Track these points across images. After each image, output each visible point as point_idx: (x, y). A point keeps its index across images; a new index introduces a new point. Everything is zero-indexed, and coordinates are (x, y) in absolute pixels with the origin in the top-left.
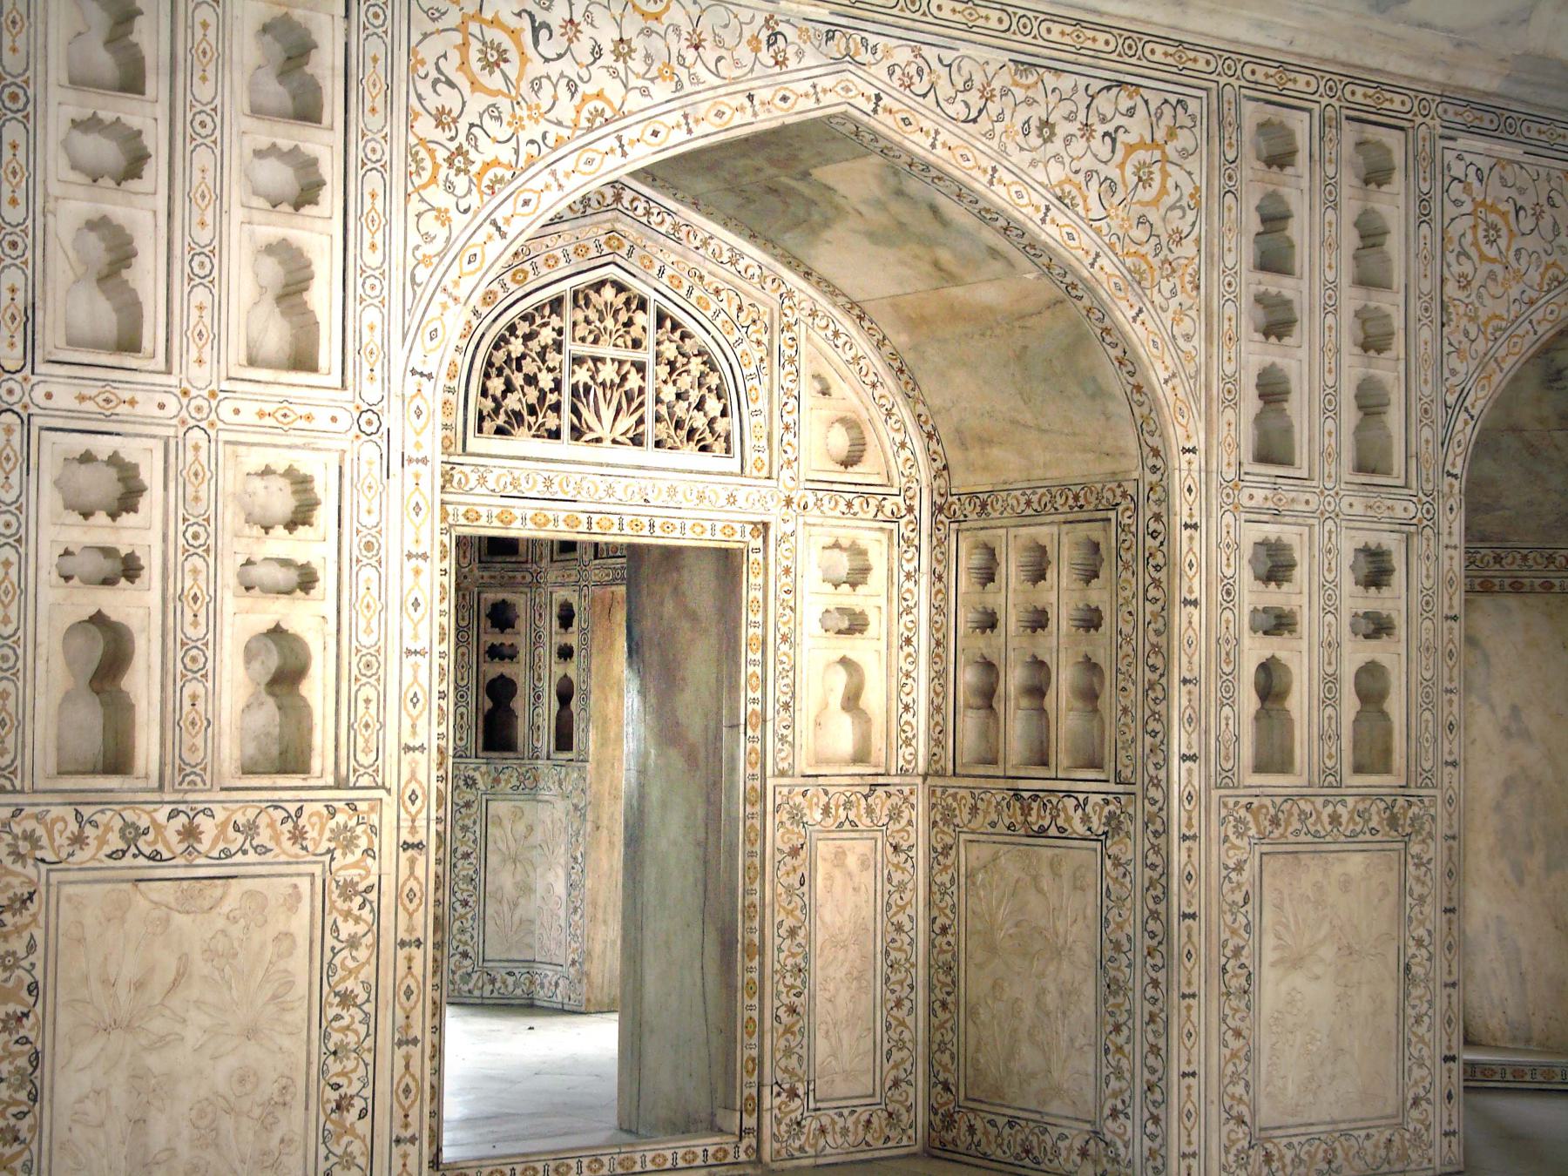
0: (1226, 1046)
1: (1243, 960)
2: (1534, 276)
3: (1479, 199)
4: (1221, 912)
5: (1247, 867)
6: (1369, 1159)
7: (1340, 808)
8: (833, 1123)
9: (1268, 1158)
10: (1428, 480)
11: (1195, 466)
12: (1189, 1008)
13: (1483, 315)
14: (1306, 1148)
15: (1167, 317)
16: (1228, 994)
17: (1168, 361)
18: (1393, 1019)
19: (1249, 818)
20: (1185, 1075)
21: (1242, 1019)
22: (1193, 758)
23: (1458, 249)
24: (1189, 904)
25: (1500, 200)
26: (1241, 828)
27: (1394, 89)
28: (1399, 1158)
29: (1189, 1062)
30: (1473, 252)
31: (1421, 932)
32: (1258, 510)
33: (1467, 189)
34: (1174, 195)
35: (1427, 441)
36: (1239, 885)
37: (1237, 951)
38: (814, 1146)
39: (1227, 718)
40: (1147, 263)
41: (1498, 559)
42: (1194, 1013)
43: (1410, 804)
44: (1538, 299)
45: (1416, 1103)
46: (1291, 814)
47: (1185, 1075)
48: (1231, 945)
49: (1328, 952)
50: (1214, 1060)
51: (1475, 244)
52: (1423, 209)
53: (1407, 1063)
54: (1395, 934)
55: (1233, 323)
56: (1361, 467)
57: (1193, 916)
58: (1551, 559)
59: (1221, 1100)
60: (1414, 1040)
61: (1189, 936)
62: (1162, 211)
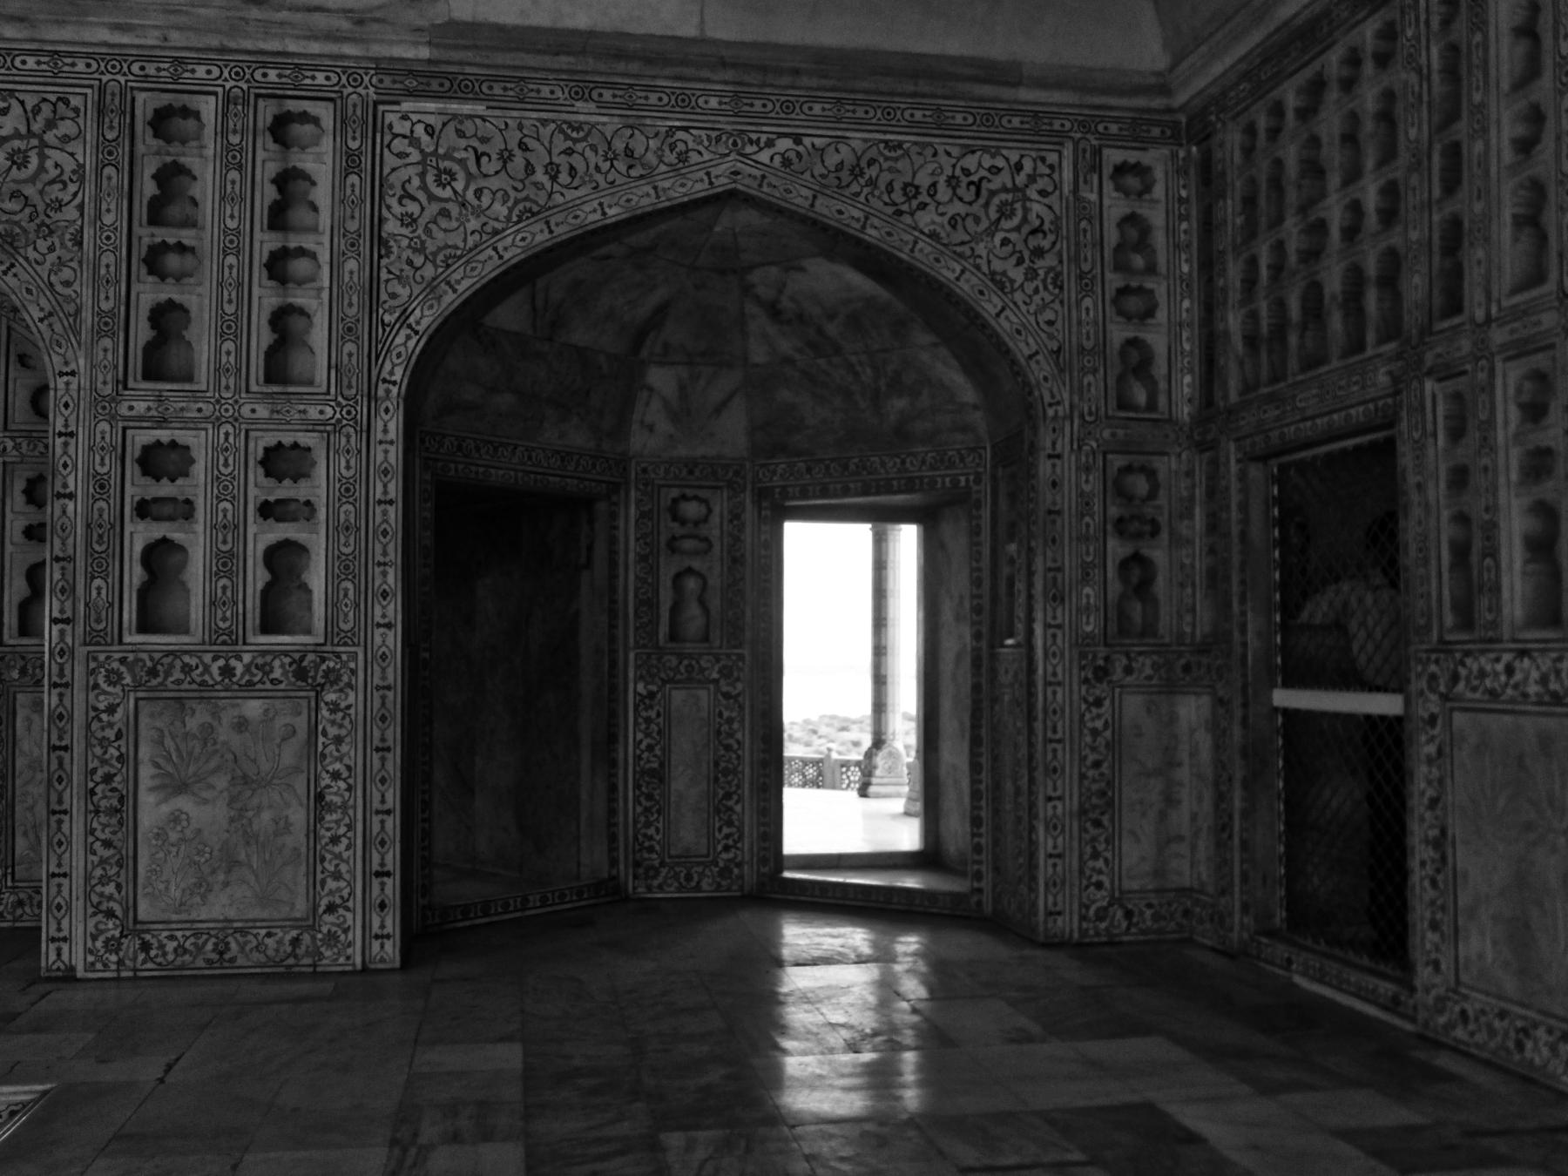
0: (94, 853)
1: (114, 785)
2: (500, 210)
3: (432, 149)
4: (88, 745)
5: (120, 710)
6: (270, 953)
7: (233, 662)
8: (30, 898)
9: (146, 947)
10: (350, 387)
11: (74, 386)
12: (60, 822)
13: (431, 247)
14: (192, 940)
15: (43, 271)
16: (97, 812)
17: (43, 302)
18: (303, 839)
19: (123, 669)
20: (54, 875)
21: (114, 833)
22: (67, 621)
23: (399, 192)
24: (60, 738)
25: (455, 149)
26: (114, 678)
27: (316, 68)
28: (307, 954)
29: (59, 865)
30: (421, 196)
31: (337, 766)
32: (140, 418)
33: (414, 141)
34: (54, 173)
35: (350, 355)
36: (111, 725)
37: (108, 778)
38: (12, 913)
39: (99, 589)
40: (21, 227)
41: (809, 470)
42: (65, 827)
43: (323, 660)
44: (504, 230)
45: (331, 908)
46: (171, 666)
47: (54, 875)
48: (100, 773)
49: (221, 782)
50: (82, 864)
51: (424, 187)
52: (350, 163)
53: (319, 876)
54: (305, 767)
55: (112, 269)
56: (269, 380)
57: (65, 748)
58: (846, 467)
59: (87, 897)
60: (329, 857)
61: (61, 764)
62: (39, 186)
